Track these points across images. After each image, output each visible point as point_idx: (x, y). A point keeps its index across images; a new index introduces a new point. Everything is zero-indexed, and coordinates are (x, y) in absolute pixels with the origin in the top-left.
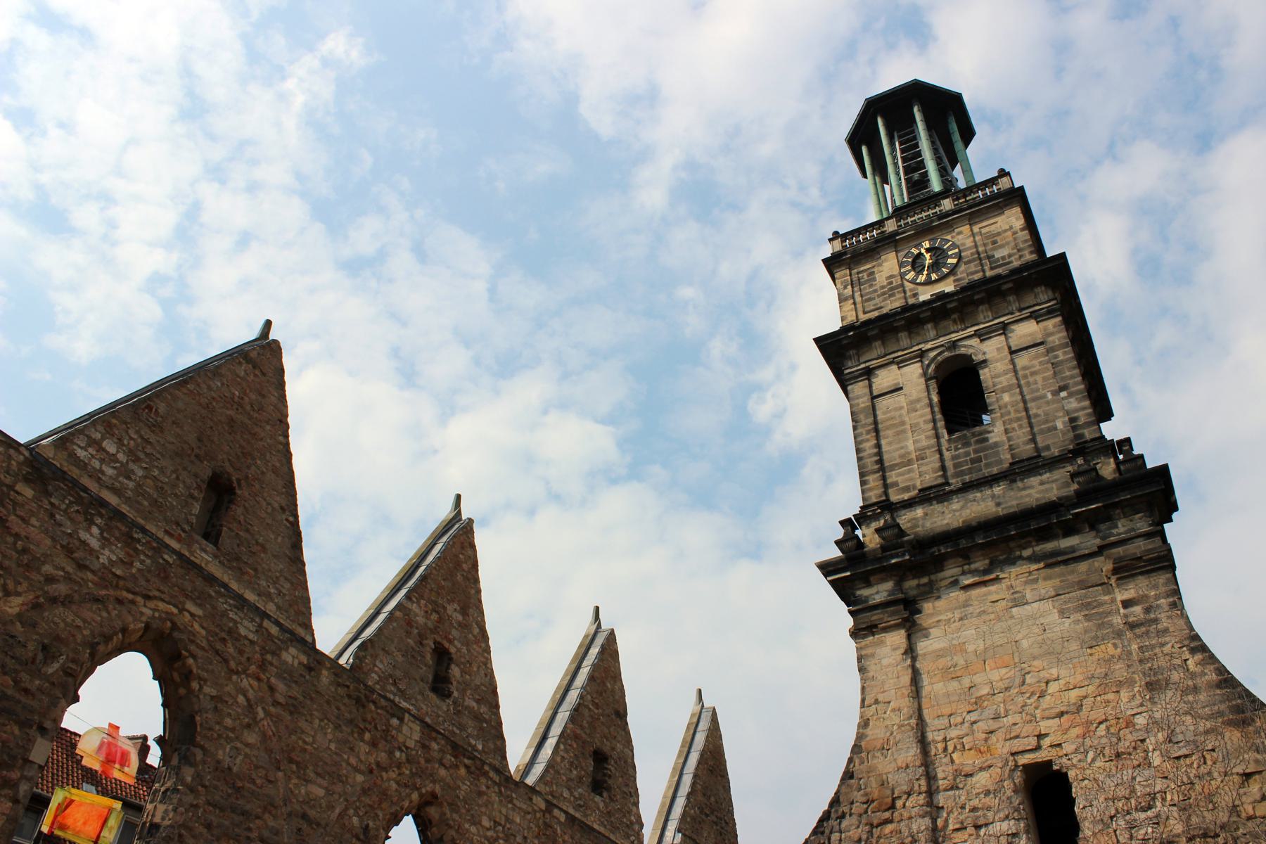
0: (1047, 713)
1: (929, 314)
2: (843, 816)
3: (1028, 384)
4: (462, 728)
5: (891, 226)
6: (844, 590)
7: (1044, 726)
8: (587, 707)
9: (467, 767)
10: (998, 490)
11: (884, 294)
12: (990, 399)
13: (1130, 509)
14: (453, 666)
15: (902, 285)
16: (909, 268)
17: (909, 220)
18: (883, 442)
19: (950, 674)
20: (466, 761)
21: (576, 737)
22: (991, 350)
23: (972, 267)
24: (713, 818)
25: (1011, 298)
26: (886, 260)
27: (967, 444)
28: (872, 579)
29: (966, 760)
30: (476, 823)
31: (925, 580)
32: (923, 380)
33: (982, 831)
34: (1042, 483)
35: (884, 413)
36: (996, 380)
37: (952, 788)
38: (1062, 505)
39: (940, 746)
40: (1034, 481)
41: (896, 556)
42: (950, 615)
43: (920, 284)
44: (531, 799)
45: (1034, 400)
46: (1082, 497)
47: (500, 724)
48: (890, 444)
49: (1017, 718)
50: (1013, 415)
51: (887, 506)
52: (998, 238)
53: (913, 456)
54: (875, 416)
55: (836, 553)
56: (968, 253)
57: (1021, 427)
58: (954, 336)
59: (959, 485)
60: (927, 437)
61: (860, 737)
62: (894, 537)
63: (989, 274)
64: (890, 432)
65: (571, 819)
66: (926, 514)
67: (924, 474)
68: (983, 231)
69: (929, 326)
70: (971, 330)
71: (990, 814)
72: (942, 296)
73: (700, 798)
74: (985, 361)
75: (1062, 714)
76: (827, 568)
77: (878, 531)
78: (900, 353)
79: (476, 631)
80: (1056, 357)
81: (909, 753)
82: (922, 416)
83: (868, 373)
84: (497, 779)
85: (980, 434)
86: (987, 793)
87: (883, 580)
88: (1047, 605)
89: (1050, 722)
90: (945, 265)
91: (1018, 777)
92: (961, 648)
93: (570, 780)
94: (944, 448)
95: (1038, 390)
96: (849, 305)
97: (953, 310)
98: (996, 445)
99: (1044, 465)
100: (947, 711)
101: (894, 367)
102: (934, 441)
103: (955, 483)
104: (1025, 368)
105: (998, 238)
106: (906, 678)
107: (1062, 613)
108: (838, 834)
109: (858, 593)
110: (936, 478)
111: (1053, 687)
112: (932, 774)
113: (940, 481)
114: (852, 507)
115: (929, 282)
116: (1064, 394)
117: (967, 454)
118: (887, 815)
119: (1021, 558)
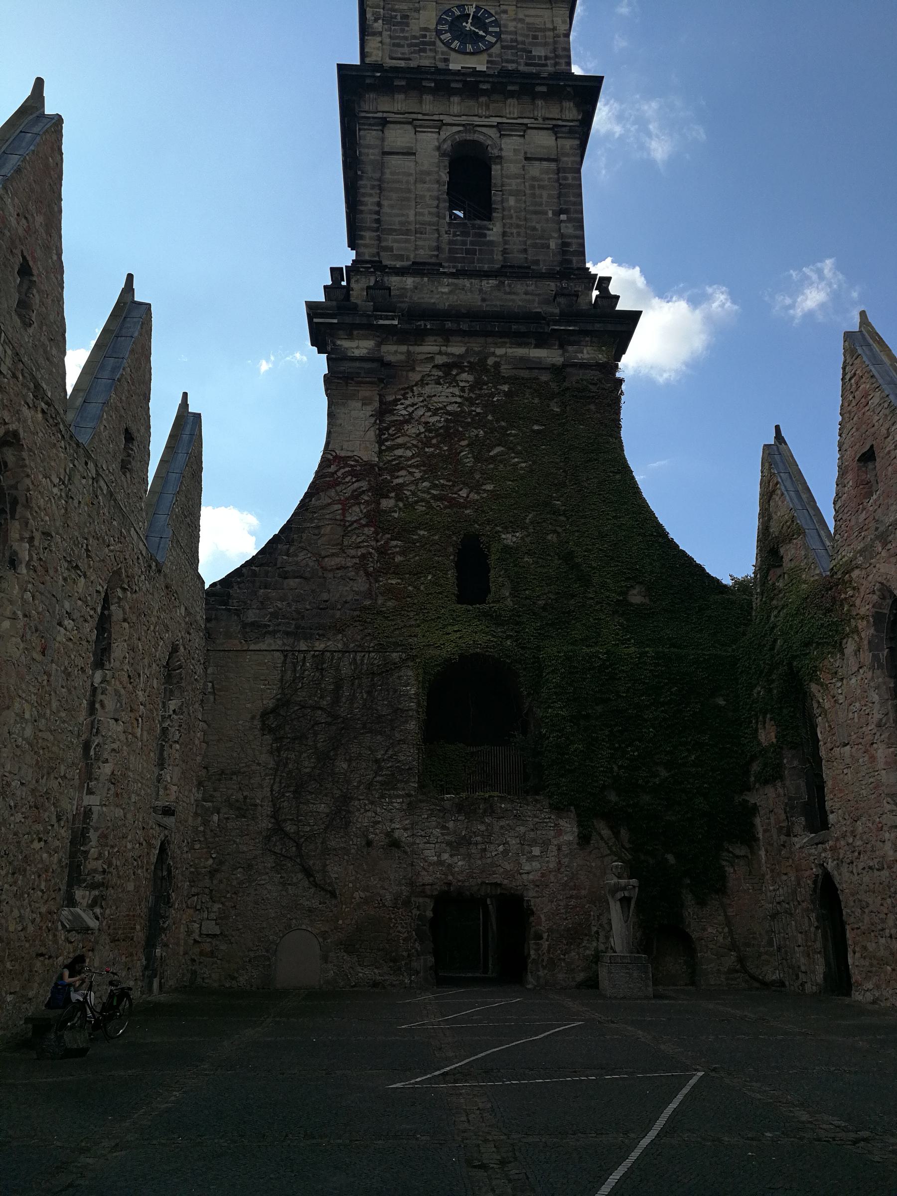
3: (533, 195)
6: (320, 338)
10: (489, 284)
11: (416, 45)
12: (496, 197)
15: (434, 43)
16: (446, 27)
18: (385, 203)
22: (510, 146)
23: (509, 54)
24: (188, 520)
25: (540, 103)
26: (425, 8)
27: (465, 234)
28: (355, 332)
32: (437, 153)
34: (526, 293)
35: (392, 173)
38: (544, 319)
40: (520, 287)
41: (387, 318)
43: (454, 50)
44: (86, 464)
45: (536, 213)
46: (568, 316)
48: (392, 207)
50: (514, 221)
51: (378, 267)
52: (540, 34)
53: (412, 227)
54: (383, 173)
56: (509, 37)
57: (519, 234)
58: (477, 120)
60: (430, 213)
63: (522, 68)
64: (394, 196)
66: (416, 288)
68: (528, 20)
69: (456, 99)
72: (474, 72)
74: (500, 157)
76: (313, 309)
77: (368, 288)
78: (420, 117)
80: (566, 179)
82: (429, 190)
83: (384, 123)
85: (480, 228)
87: (366, 338)
94: (443, 231)
95: (541, 205)
97: (485, 93)
98: (491, 243)
99: (533, 277)
101: (409, 127)
102: (435, 219)
104: (534, 179)
105: (540, 34)
108: (285, 557)
109: (339, 342)
113: (433, 260)
114: (346, 257)
116: (563, 217)
117: (464, 243)
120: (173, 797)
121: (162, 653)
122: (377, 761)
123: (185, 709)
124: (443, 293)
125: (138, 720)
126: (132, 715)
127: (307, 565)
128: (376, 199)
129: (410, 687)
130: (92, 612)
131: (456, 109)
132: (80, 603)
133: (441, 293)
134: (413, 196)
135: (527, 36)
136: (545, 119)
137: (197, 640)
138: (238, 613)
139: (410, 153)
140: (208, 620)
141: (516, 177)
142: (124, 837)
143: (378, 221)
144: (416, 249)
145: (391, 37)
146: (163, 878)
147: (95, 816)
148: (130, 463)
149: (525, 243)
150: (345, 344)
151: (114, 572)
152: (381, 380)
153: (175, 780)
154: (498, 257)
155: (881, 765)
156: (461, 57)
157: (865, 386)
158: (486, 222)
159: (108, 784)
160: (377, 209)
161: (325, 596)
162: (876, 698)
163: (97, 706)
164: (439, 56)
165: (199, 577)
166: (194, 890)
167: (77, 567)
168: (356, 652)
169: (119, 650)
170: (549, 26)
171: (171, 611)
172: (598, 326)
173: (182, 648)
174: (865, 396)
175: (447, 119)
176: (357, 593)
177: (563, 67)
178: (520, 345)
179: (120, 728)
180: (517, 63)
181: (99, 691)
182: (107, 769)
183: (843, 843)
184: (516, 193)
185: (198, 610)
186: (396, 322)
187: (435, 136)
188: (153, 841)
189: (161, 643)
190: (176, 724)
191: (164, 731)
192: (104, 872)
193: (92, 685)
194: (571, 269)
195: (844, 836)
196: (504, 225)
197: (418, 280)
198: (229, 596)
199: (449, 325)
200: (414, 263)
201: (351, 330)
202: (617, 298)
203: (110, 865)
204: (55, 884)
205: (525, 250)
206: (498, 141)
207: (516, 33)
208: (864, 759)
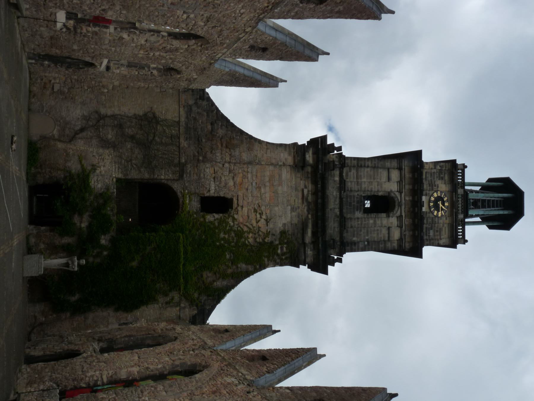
0: (250, 211)
1: (416, 200)
2: (227, 127)
3: (374, 231)
4: (286, 5)
5: (460, 191)
6: (314, 142)
7: (245, 209)
8: (287, 48)
9: (268, 7)
10: (337, 211)
12: (373, 215)
13: (316, 257)
14: (314, 5)
15: (432, 190)
16: (439, 195)
17: (460, 199)
18: (369, 169)
19: (272, 177)
20: (270, 7)
21: (274, 43)
22: (393, 221)
23: (430, 220)
25: (411, 233)
27: (358, 202)
29: (238, 179)
30: (243, 7)
31: (310, 176)
32: (389, 190)
33: (213, 180)
34: (334, 227)
36: (380, 219)
37: (230, 171)
39: (246, 170)
40: (336, 225)
42: (294, 183)
47: (285, 18)
48: (367, 172)
49: (250, 200)
50: (364, 222)
52: (438, 233)
53: (359, 180)
54: (381, 168)
55: (329, 142)
57: (358, 224)
58: (403, 207)
59: (342, 196)
61: (256, 139)
62: (329, 166)
63: (425, 226)
65: (239, 39)
66: (335, 181)
67: (351, 184)
68: (444, 228)
69: (411, 198)
70: (403, 214)
71: (218, 183)
73: (242, 78)
75: (248, 217)
78: (403, 184)
79: (328, 15)
80: (382, 244)
81: (245, 157)
83: (400, 169)
84: (261, 16)
86: (226, 184)
88: (289, 219)
89: (246, 212)
90: (434, 210)
91: (229, 196)
92: (280, 184)
93: (257, 39)
94: (359, 193)
96: (432, 166)
98: (354, 213)
100: (259, 175)
101: (399, 179)
102: (363, 189)
103: (344, 195)
104: (381, 231)
105: (438, 233)
106: (274, 161)
107: (284, 225)
110: (348, 188)
111: (258, 216)
112: (236, 165)
113: (346, 189)
115: (430, 201)
116: (366, 243)
117: (354, 202)
118: (224, 145)
119: (309, 213)
120: (115, 71)
121: (177, 65)
122: (131, 160)
123: (153, 77)
124: (333, 192)
125: (147, 51)
126: (148, 49)
127: (217, 133)
128: (370, 165)
129: (164, 175)
130: (190, 28)
131: (407, 198)
132: (194, 22)
133: (332, 192)
134: (372, 180)
135: (437, 228)
136: (405, 235)
137: (183, 84)
138: (196, 103)
139: (389, 179)
140: (193, 90)
141: (382, 223)
142: (96, 44)
143: (361, 166)
144: (351, 182)
145: (434, 172)
146: (78, 65)
147: (105, 30)
148: (254, 50)
149: (355, 227)
150: (311, 152)
151: (208, 41)
152: (296, 166)
153: (122, 72)
154: (349, 216)
155: (129, 369)
156: (428, 201)
157: (294, 356)
158: (362, 211)
159: (119, 36)
160: (366, 165)
161: (204, 140)
162: (160, 366)
163: (152, 33)
164: (428, 192)
165: (210, 86)
166: (73, 81)
167: (208, 21)
168: (179, 152)
169: (176, 43)
170: (442, 237)
171: (194, 70)
172: (321, 257)
173: (179, 76)
174: (290, 356)
175: (403, 195)
176: (206, 154)
177: (426, 243)
178: (313, 225)
179: (143, 42)
180: (427, 224)
181: (159, 34)
182: (125, 36)
183: (94, 358)
184: (375, 223)
185: (197, 85)
186: (320, 172)
187: (396, 190)
188: (95, 59)
189: (181, 65)
190: (146, 73)
191: (143, 68)
192: (81, 33)
193: (161, 31)
194: (345, 246)
195: (98, 359)
196: (362, 218)
197: (338, 182)
198: (203, 100)
199: (320, 194)
200: (345, 181)
201: (315, 153)
202: (333, 265)
203: (84, 36)
204: (76, 8)
205: (352, 227)
206: (396, 216)
207: (438, 223)
208: (132, 364)
